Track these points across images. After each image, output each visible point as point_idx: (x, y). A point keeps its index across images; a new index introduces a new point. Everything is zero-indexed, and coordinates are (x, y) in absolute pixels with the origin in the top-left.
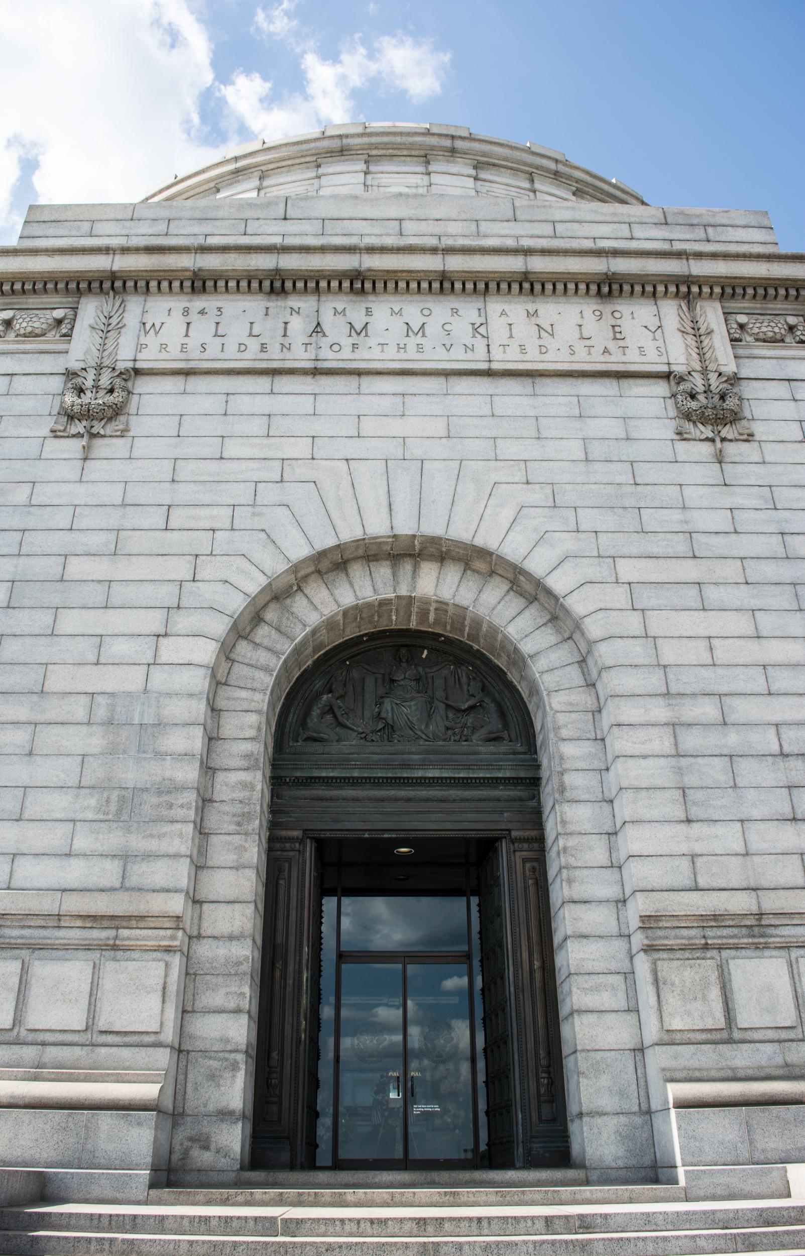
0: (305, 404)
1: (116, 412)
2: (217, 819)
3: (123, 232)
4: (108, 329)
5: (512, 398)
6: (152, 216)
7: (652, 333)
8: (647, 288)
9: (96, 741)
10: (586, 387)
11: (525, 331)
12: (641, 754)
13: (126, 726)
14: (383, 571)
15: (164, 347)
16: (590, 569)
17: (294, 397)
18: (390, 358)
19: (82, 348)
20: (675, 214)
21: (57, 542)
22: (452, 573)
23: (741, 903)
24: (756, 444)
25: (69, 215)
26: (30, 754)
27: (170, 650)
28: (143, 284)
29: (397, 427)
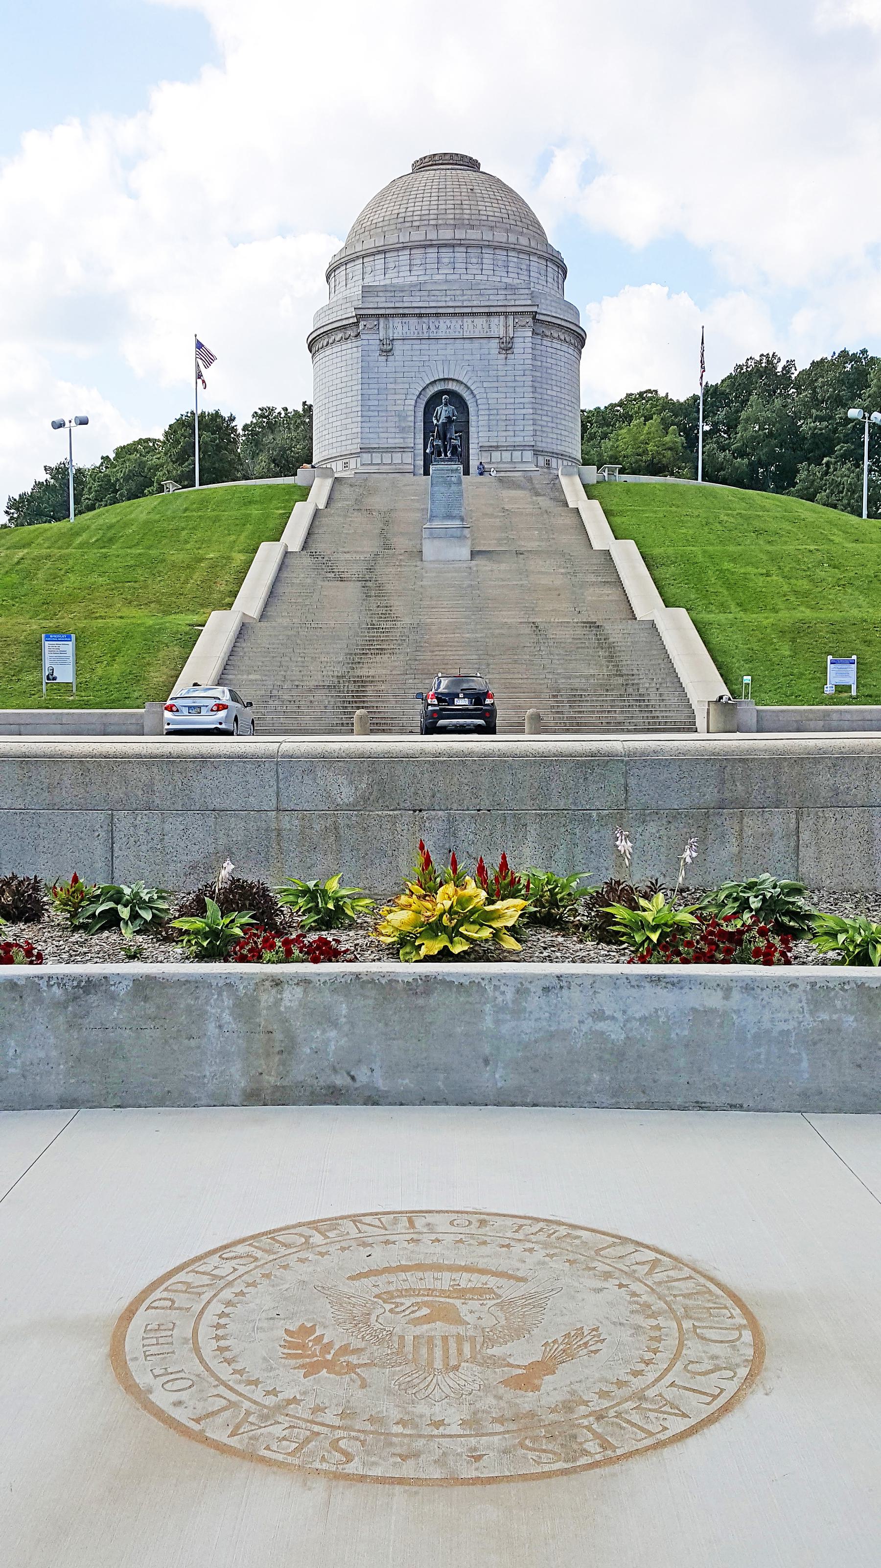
0: (426, 347)
1: (391, 350)
2: (417, 430)
4: (386, 328)
5: (467, 345)
7: (497, 327)
8: (497, 314)
9: (397, 419)
10: (481, 341)
14: (442, 383)
16: (479, 385)
17: (425, 345)
18: (443, 335)
21: (385, 380)
22: (455, 384)
23: (495, 444)
28: (393, 316)
29: (444, 352)
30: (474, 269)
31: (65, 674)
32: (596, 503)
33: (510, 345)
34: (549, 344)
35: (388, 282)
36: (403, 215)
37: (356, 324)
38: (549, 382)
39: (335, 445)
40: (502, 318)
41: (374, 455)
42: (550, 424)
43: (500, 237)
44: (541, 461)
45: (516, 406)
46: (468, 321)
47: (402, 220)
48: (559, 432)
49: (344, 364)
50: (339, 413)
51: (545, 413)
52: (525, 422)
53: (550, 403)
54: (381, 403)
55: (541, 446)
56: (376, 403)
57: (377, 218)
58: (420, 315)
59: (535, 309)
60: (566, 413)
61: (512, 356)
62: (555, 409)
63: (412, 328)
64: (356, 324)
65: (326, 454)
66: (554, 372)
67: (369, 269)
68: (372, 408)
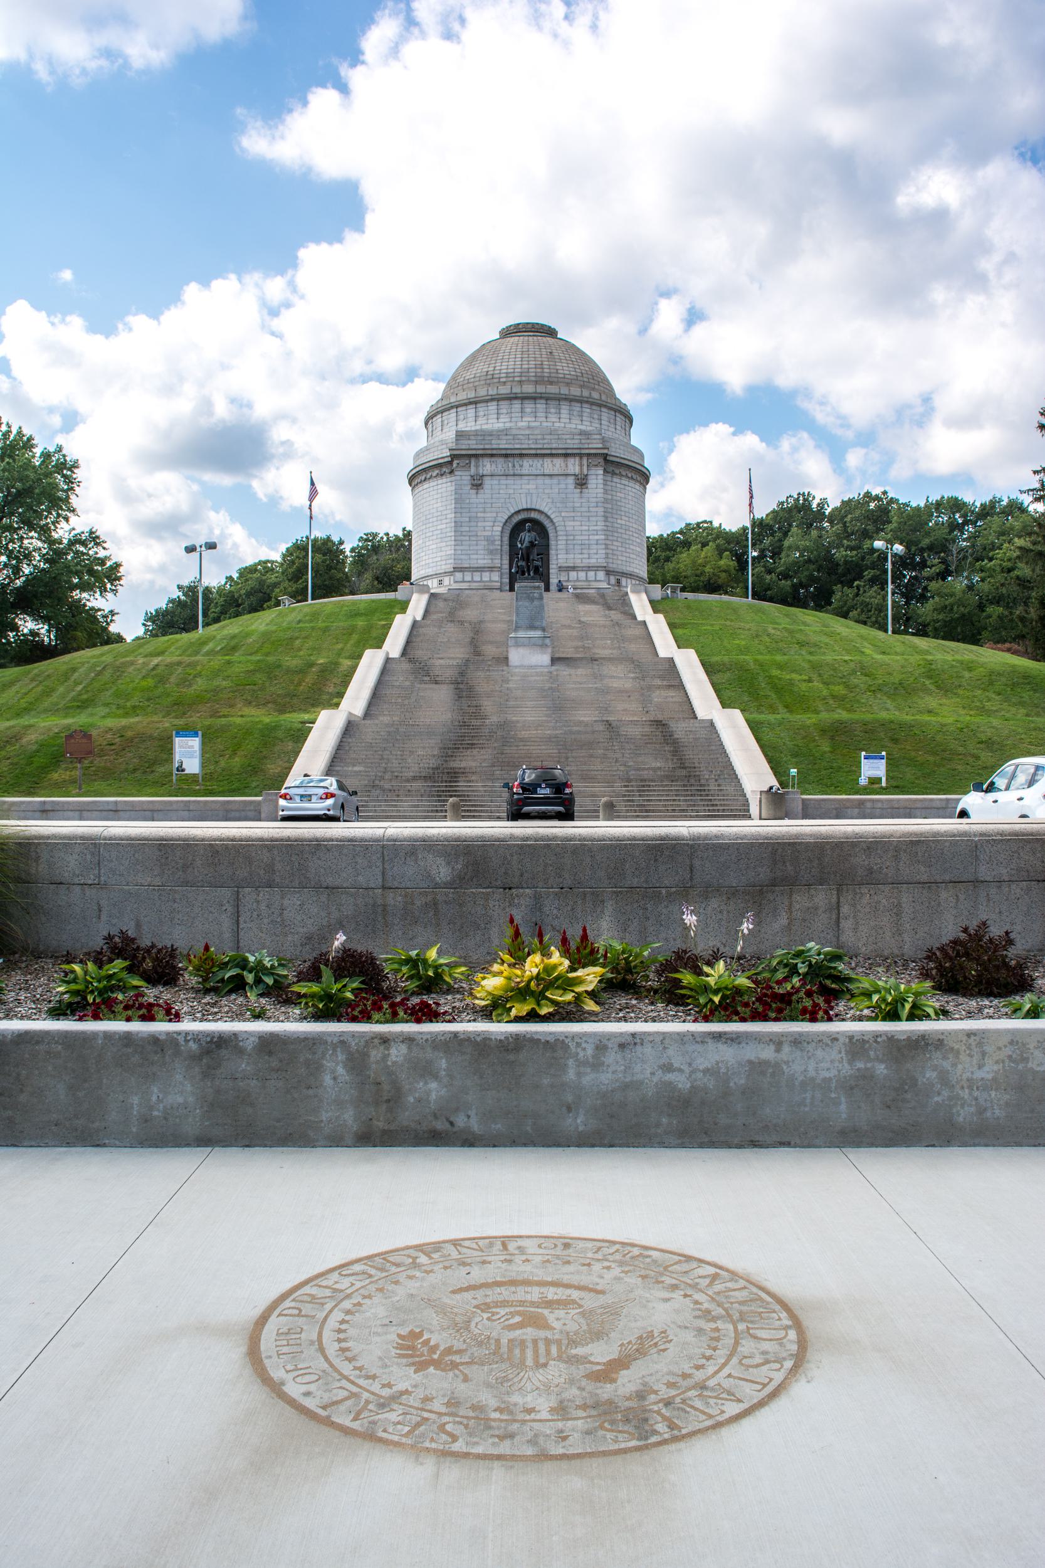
4: (477, 466)
5: (548, 481)
7: (573, 466)
8: (574, 455)
11: (550, 465)
12: (562, 544)
13: (490, 540)
17: (510, 481)
18: (526, 472)
19: (473, 470)
27: (495, 528)
28: (483, 455)
30: (553, 418)
31: (192, 766)
32: (661, 617)
35: (478, 427)
37: (451, 463)
40: (577, 459)
43: (575, 391)
44: (613, 580)
46: (548, 462)
55: (612, 566)
57: (469, 375)
58: (506, 456)
59: (606, 451)
63: (500, 466)
64: (451, 463)
65: (423, 573)
67: (462, 417)
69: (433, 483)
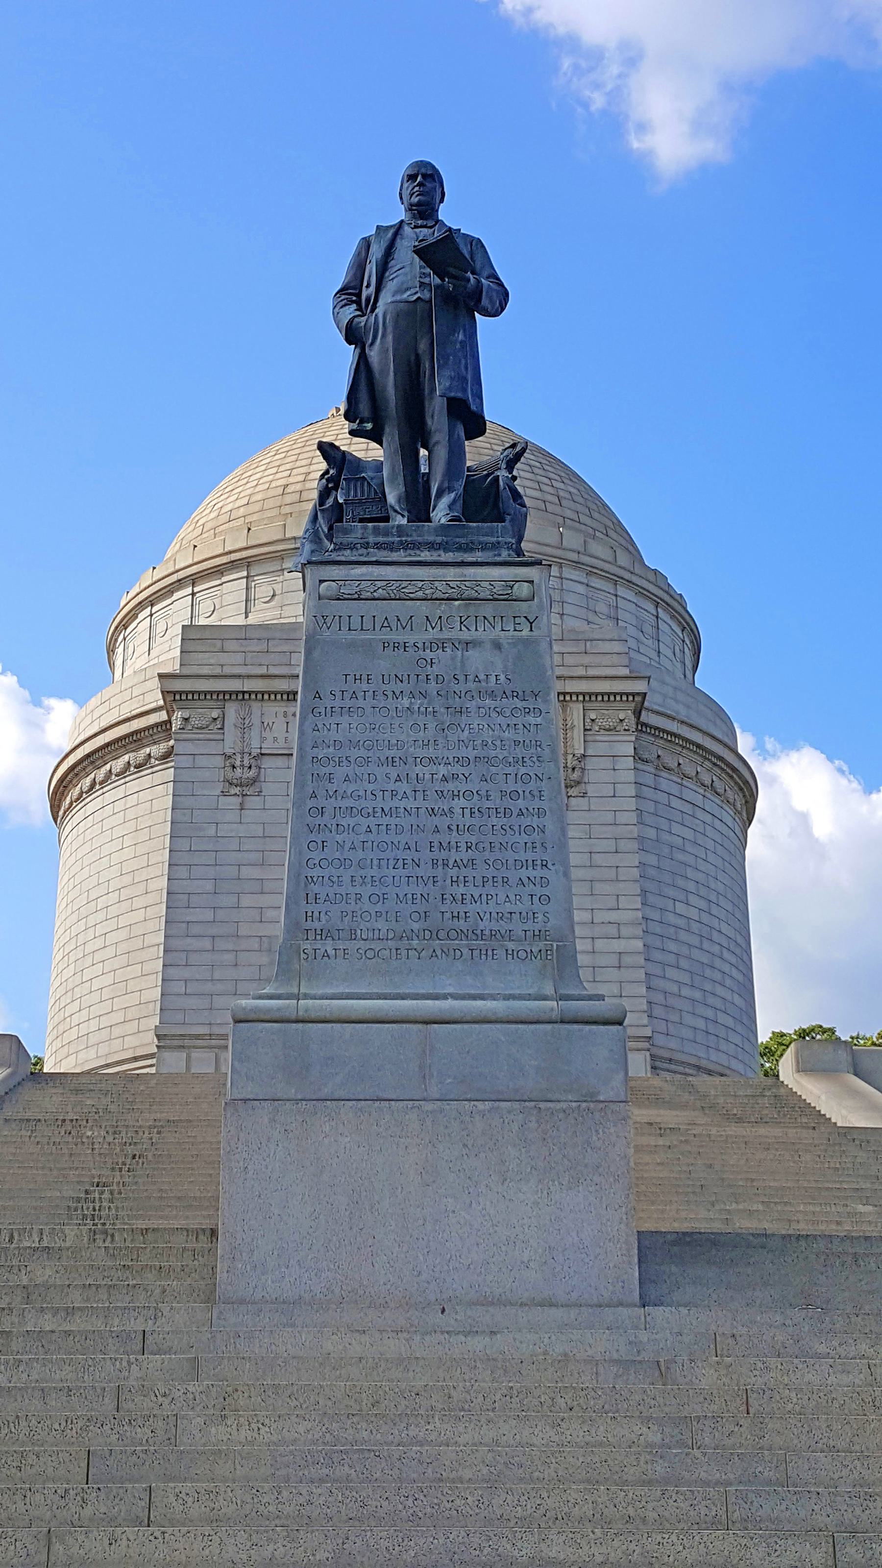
3: (243, 649)
4: (244, 728)
6: (258, 636)
15: (275, 739)
19: (231, 741)
20: (569, 631)
24: (587, 799)
25: (207, 635)
26: (236, 965)
28: (261, 696)
33: (575, 776)
34: (675, 789)
36: (298, 487)
38: (681, 882)
39: (93, 1039)
41: (195, 1054)
42: (686, 991)
45: (598, 931)
47: (296, 497)
48: (710, 1013)
49: (131, 826)
50: (110, 952)
51: (671, 959)
52: (626, 974)
53: (683, 936)
54: (221, 915)
56: (209, 915)
59: (639, 686)
60: (726, 968)
61: (582, 803)
62: (696, 954)
66: (691, 860)
68: (195, 929)
69: (113, 793)
